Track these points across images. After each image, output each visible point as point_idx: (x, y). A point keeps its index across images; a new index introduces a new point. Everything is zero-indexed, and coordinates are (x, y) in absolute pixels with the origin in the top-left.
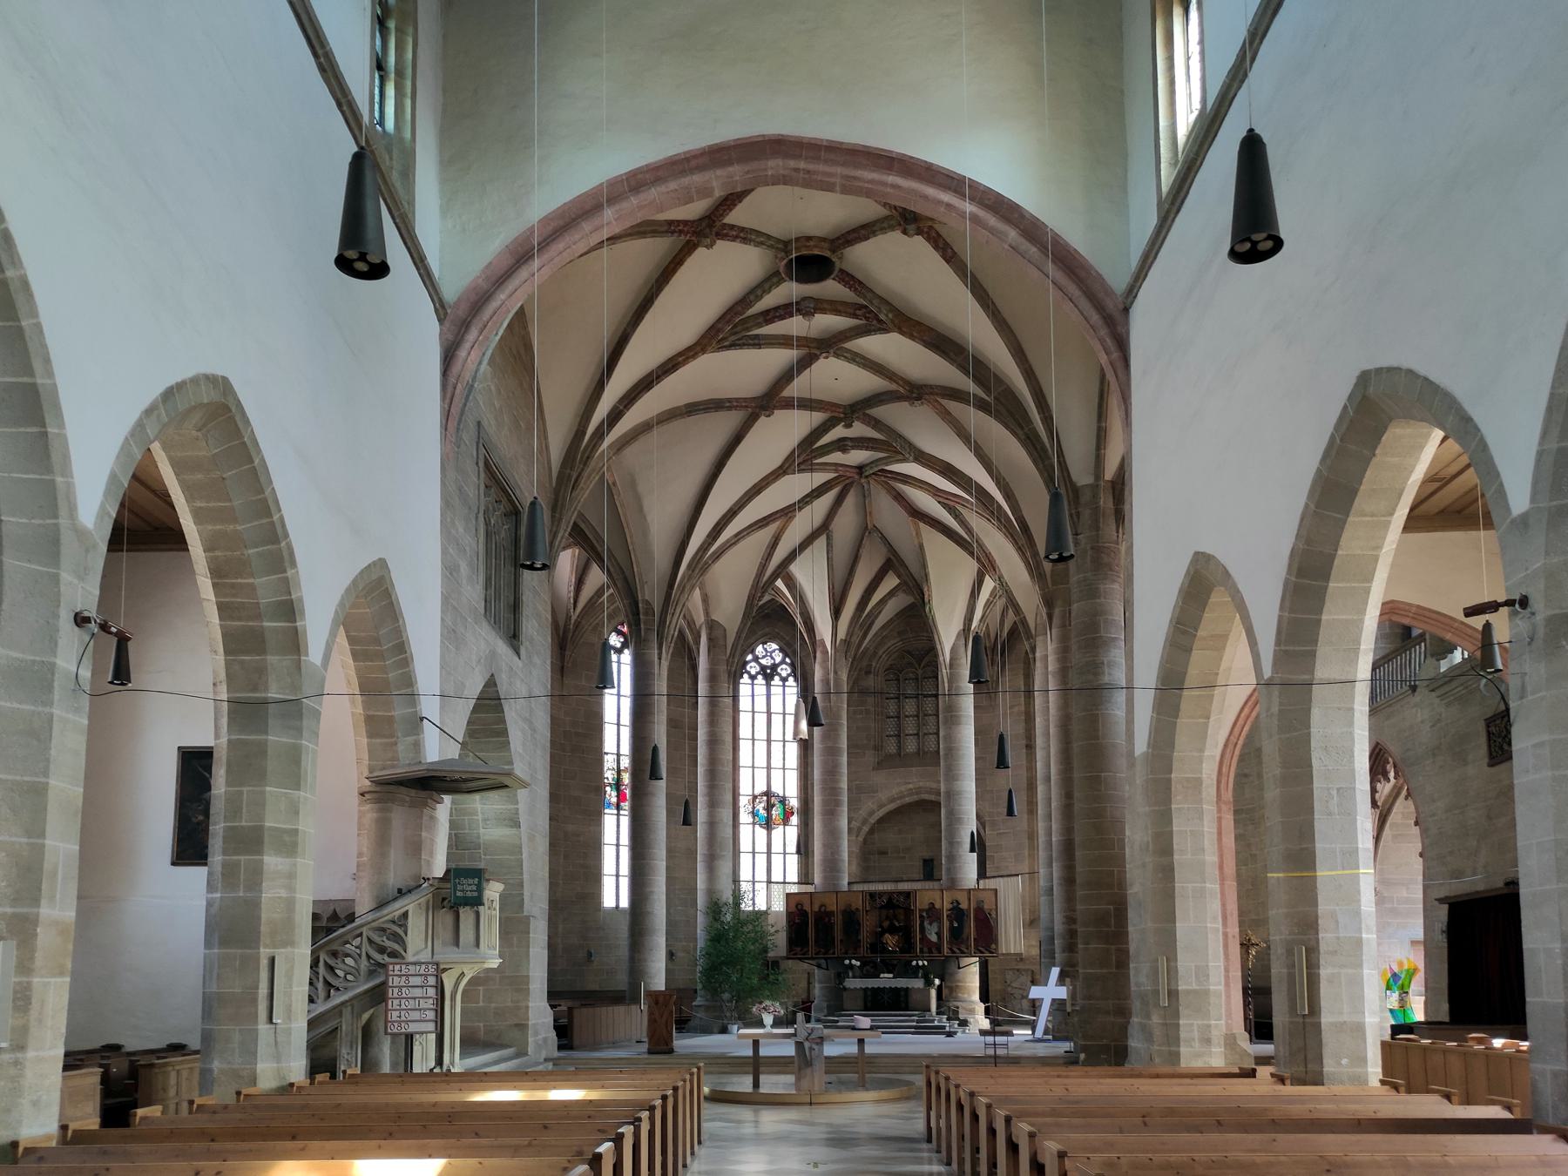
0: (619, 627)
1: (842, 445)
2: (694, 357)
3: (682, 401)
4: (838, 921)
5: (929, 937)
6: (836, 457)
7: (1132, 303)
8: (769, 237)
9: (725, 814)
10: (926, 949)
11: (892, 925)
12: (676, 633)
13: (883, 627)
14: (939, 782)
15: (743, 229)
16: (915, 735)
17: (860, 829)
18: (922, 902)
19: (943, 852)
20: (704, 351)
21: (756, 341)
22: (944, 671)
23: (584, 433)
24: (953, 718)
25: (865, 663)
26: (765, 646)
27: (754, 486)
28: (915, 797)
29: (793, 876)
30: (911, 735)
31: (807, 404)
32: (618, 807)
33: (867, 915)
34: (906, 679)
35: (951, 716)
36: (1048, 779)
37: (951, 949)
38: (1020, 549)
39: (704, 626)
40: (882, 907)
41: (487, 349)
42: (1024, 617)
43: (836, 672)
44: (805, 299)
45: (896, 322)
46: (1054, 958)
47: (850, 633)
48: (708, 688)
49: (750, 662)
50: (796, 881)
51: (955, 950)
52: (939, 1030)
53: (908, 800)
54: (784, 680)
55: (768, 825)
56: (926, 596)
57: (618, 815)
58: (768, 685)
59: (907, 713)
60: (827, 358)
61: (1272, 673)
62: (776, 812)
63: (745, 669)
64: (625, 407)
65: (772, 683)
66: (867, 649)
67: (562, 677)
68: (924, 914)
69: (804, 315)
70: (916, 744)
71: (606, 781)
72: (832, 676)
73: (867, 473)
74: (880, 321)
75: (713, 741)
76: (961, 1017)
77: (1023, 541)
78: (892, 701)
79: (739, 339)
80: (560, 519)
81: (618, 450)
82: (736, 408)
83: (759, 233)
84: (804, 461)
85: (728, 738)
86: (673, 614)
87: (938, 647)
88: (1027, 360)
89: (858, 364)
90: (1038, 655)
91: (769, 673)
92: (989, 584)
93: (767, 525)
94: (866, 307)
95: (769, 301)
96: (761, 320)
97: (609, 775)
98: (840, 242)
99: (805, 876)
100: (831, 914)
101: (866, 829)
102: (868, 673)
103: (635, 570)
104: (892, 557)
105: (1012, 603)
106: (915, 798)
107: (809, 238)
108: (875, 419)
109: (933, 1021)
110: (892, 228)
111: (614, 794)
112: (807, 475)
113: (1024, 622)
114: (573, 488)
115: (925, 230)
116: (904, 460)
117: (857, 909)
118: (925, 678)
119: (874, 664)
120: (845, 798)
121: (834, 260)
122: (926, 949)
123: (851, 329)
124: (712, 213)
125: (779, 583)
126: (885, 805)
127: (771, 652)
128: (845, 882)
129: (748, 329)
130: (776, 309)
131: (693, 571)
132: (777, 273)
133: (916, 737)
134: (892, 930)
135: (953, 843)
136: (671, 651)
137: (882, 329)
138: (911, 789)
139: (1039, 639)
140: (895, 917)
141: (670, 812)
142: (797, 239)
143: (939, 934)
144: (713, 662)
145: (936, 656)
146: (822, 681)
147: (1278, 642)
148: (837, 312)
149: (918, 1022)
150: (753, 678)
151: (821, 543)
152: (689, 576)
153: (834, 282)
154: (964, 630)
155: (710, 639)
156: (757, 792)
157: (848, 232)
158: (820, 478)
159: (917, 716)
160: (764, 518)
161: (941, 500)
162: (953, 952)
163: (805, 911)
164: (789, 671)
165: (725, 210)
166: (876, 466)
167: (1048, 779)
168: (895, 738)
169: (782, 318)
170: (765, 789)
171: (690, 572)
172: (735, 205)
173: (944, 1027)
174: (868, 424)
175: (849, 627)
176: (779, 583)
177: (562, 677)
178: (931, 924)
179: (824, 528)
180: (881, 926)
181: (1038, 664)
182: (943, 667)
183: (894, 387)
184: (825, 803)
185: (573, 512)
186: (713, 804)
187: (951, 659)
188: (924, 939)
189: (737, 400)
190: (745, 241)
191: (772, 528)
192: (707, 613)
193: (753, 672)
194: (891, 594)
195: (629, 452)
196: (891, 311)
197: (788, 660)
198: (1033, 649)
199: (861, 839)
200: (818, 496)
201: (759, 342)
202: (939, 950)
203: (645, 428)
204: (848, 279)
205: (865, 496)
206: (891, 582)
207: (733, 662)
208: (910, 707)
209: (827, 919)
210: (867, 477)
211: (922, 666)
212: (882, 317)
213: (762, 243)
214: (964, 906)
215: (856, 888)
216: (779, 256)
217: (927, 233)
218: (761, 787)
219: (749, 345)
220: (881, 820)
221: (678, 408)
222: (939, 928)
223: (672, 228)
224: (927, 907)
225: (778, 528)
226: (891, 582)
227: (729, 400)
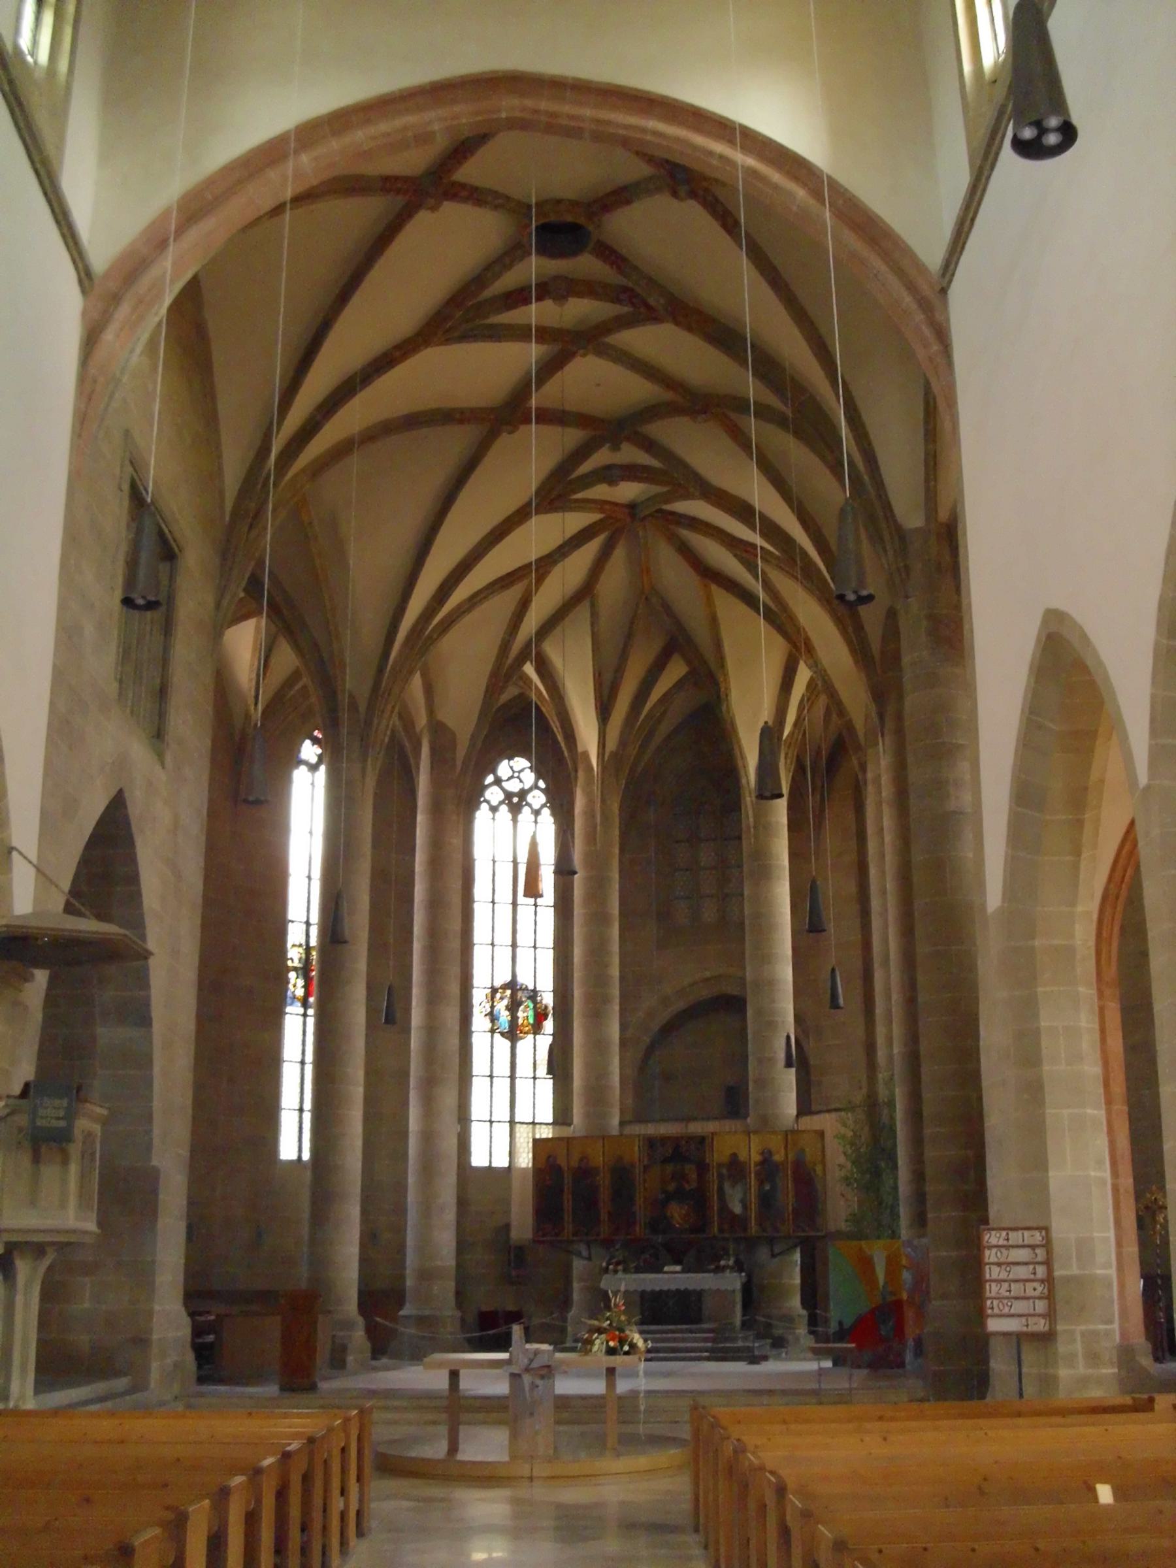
1: (609, 475)
5: (730, 1205)
6: (600, 491)
7: (950, 281)
9: (451, 1015)
22: (748, 799)
24: (764, 873)
29: (546, 1113)
32: (305, 1004)
39: (425, 731)
40: (666, 1161)
42: (850, 721)
43: (603, 801)
44: (557, 278)
47: (623, 743)
50: (551, 1121)
54: (537, 813)
55: (513, 1034)
57: (305, 1015)
58: (515, 820)
60: (584, 355)
61: (1149, 780)
65: (520, 817)
68: (724, 1171)
71: (290, 963)
76: (777, 1332)
85: (456, 900)
87: (740, 763)
90: (869, 775)
91: (515, 803)
92: (803, 675)
94: (632, 290)
95: (509, 280)
97: (294, 955)
99: (562, 1115)
105: (836, 705)
110: (658, 190)
111: (301, 982)
113: (850, 727)
116: (687, 496)
120: (616, 992)
128: (616, 1121)
135: (766, 1061)
137: (650, 316)
139: (870, 751)
141: (371, 1011)
144: (437, 782)
145: (737, 780)
146: (585, 813)
147: (1154, 732)
149: (714, 1340)
150: (494, 809)
151: (582, 613)
156: (497, 984)
170: (508, 978)
179: (585, 592)
181: (870, 789)
182: (747, 794)
183: (669, 396)
184: (590, 998)
186: (434, 999)
191: (516, 592)
192: (431, 711)
197: (542, 784)
198: (863, 768)
204: (609, 254)
208: (706, 856)
212: (652, 301)
214: (778, 1157)
218: (503, 977)
222: (745, 1194)
226: (676, 670)
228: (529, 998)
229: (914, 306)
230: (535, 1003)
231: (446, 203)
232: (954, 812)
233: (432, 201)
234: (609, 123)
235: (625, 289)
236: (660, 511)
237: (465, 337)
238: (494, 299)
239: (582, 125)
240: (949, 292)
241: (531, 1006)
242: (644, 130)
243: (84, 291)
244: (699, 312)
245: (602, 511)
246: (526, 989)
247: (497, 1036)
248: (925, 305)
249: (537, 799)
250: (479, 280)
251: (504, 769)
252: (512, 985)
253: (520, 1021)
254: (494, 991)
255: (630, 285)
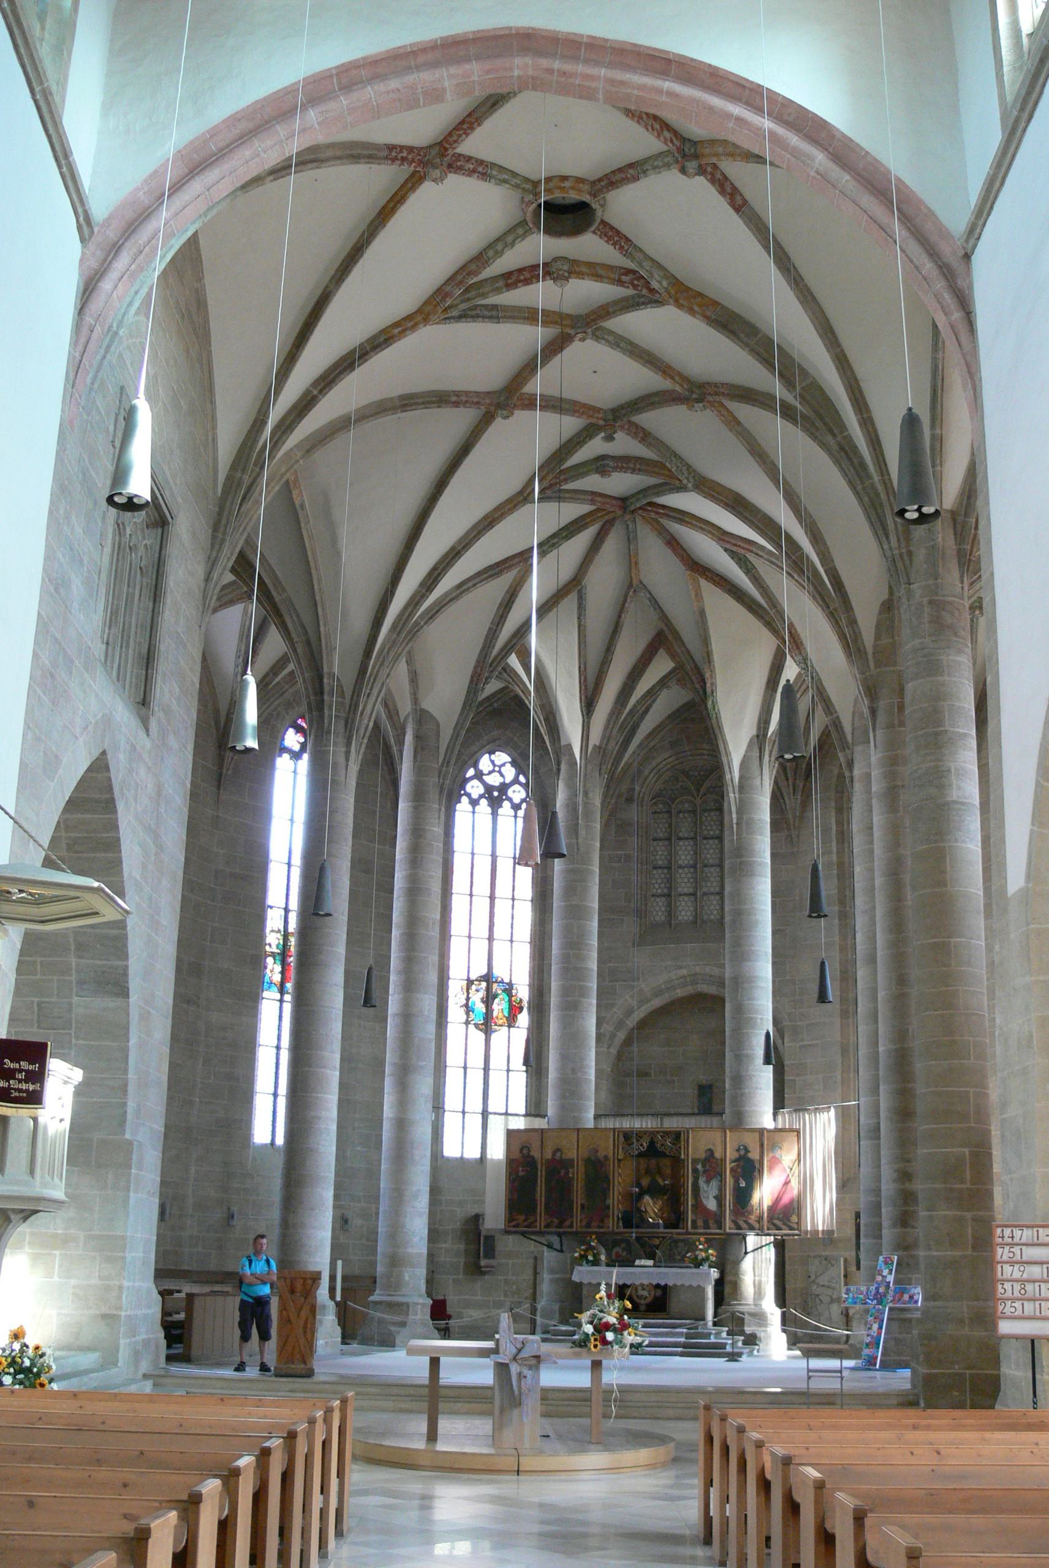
0: (299, 721)
1: (601, 465)
2: (414, 327)
3: (396, 390)
4: (578, 1176)
5: (704, 1201)
6: (592, 482)
8: (514, 174)
10: (700, 1223)
11: (654, 1182)
12: (371, 724)
13: (651, 735)
14: (723, 966)
15: (481, 162)
16: (691, 894)
17: (613, 1036)
18: (695, 1148)
19: (727, 1070)
20: (426, 321)
21: (494, 313)
22: (731, 795)
23: (264, 423)
24: (743, 868)
25: (624, 788)
26: (493, 757)
27: (485, 518)
28: (690, 988)
29: (519, 1104)
30: (685, 894)
31: (555, 404)
32: (282, 990)
33: (619, 1166)
34: (680, 812)
35: (741, 863)
36: (872, 959)
37: (735, 1222)
38: (832, 615)
39: (410, 719)
40: (641, 1155)
41: (141, 287)
42: (838, 717)
43: (586, 793)
44: (556, 259)
45: (672, 292)
46: (880, 1237)
47: (606, 736)
48: (411, 810)
49: (472, 778)
50: (523, 1112)
51: (741, 1223)
52: (715, 1350)
53: (680, 993)
55: (487, 1026)
56: (708, 685)
57: (281, 1001)
58: (495, 814)
59: (680, 862)
60: (583, 340)
62: (500, 1007)
63: (464, 789)
64: (321, 391)
65: (500, 811)
66: (629, 765)
67: (219, 789)
68: (699, 1167)
69: (555, 280)
70: (692, 909)
71: (268, 948)
72: (580, 799)
73: (633, 508)
74: (652, 291)
75: (415, 890)
76: (748, 1330)
77: (836, 604)
78: (661, 843)
79: (470, 309)
80: (223, 541)
81: (308, 451)
82: (465, 404)
83: (501, 168)
84: (551, 486)
85: (436, 887)
86: (369, 695)
87: (724, 759)
88: (839, 345)
89: (623, 351)
92: (791, 671)
93: (499, 574)
95: (510, 260)
96: (501, 283)
97: (273, 941)
98: (602, 184)
99: (535, 1108)
100: (570, 1163)
101: (621, 1036)
102: (629, 800)
103: (322, 629)
104: (665, 629)
106: (689, 990)
107: (564, 178)
108: (643, 429)
109: (708, 1336)
110: (668, 166)
112: (554, 505)
113: (837, 724)
114: (244, 498)
115: (709, 169)
117: (606, 1158)
118: (705, 811)
119: (637, 788)
120: (593, 985)
121: (594, 206)
122: (700, 1223)
123: (615, 303)
124: (444, 138)
125: (513, 661)
126: (648, 1000)
127: (500, 767)
129: (484, 295)
130: (520, 271)
131: (399, 634)
132: (523, 223)
133: (692, 898)
134: (654, 1191)
135: (741, 1058)
136: (362, 750)
138: (684, 977)
139: (858, 749)
140: (660, 1172)
142: (548, 180)
143: (720, 1199)
144: (419, 770)
145: (721, 778)
146: (567, 805)
148: (598, 277)
150: (474, 803)
152: (391, 643)
153: (594, 236)
154: (758, 736)
155: (418, 737)
157: (613, 172)
158: (572, 511)
159: (694, 867)
160: (497, 564)
161: (728, 546)
162: (739, 1228)
163: (533, 1157)
164: (523, 794)
165: (460, 136)
166: (645, 497)
167: (872, 959)
168: (663, 899)
169: (527, 282)
170: (484, 971)
171: (395, 636)
172: (473, 129)
173: (723, 1346)
174: (635, 435)
175: (606, 728)
176: (513, 661)
177: (219, 789)
178: (708, 1182)
180: (639, 1185)
181: (857, 786)
182: (730, 789)
184: (566, 991)
185: (242, 534)
187: (741, 777)
188: (698, 1206)
189: (467, 393)
190: (485, 176)
192: (416, 701)
193: (475, 796)
194: (663, 683)
195: (319, 455)
196: (667, 278)
198: (850, 764)
199: (614, 1051)
200: (568, 537)
201: (496, 314)
202: (720, 1224)
203: (341, 425)
204: (613, 235)
205: (631, 539)
206: (661, 666)
207: (447, 772)
209: (563, 1172)
210: (633, 512)
211: (702, 791)
212: (654, 284)
213: (505, 181)
215: (609, 1123)
216: (526, 200)
217: (711, 174)
219: (484, 317)
220: (643, 1024)
221: (391, 399)
223: (394, 154)
224: (703, 1156)
225: (515, 579)
226: (661, 666)
227: (457, 394)
228: (504, 991)
229: (935, 273)
230: (510, 995)
231: (450, 175)
232: (954, 802)
233: (436, 173)
234: (623, 83)
235: (629, 271)
236: (651, 504)
237: (463, 317)
238: (495, 279)
239: (594, 85)
240: (973, 258)
241: (507, 999)
242: (659, 91)
243: (83, 240)
244: (700, 295)
245: (593, 502)
246: (502, 982)
247: (471, 1027)
248: (947, 272)
249: (517, 793)
250: (480, 259)
251: (485, 763)
252: (488, 978)
253: (495, 1014)
254: (470, 983)
255: (633, 266)
